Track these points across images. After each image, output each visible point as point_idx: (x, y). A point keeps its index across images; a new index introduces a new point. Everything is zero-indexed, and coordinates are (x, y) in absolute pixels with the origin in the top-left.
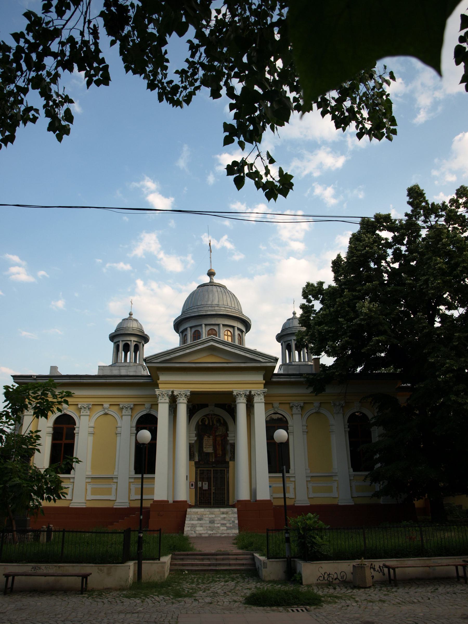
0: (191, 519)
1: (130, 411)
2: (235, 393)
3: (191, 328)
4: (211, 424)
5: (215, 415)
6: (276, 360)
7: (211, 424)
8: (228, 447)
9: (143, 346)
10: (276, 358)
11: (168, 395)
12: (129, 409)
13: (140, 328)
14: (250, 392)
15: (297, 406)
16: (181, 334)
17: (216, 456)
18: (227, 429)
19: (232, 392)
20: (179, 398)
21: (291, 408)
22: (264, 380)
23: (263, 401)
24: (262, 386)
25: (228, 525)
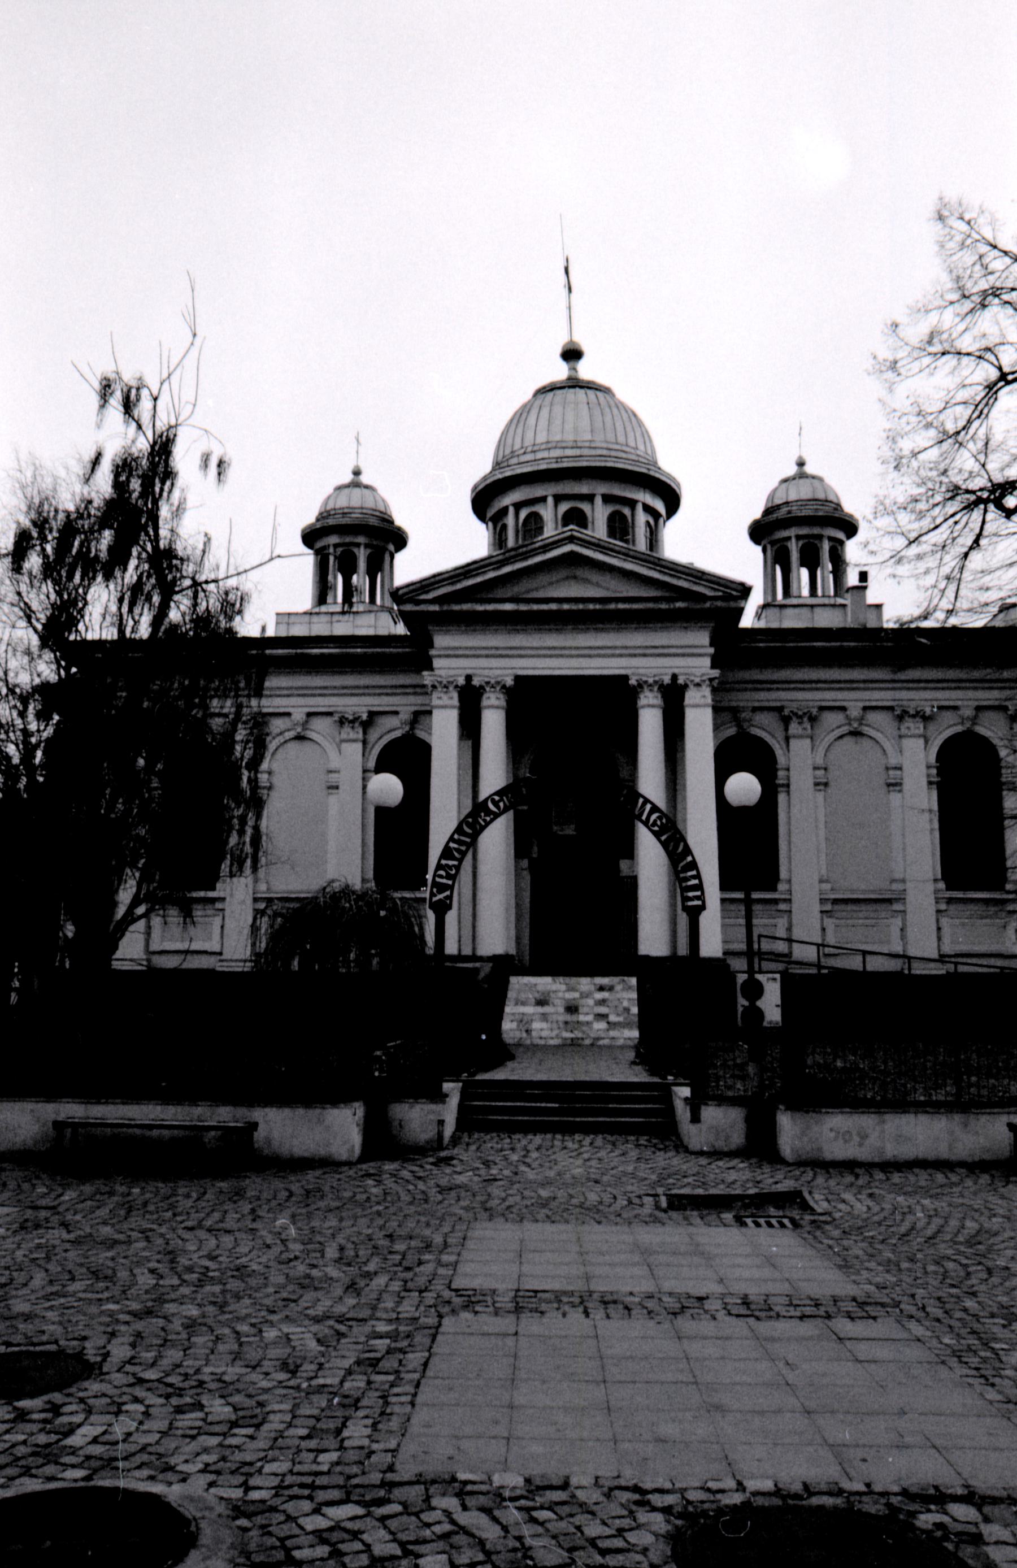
0: (518, 1002)
1: (361, 731)
2: (633, 682)
3: (518, 506)
6: (745, 591)
9: (392, 557)
10: (742, 584)
12: (357, 725)
13: (382, 509)
14: (674, 677)
15: (800, 717)
16: (490, 524)
19: (626, 678)
20: (485, 696)
21: (786, 721)
23: (709, 700)
24: (707, 662)
25: (613, 1018)
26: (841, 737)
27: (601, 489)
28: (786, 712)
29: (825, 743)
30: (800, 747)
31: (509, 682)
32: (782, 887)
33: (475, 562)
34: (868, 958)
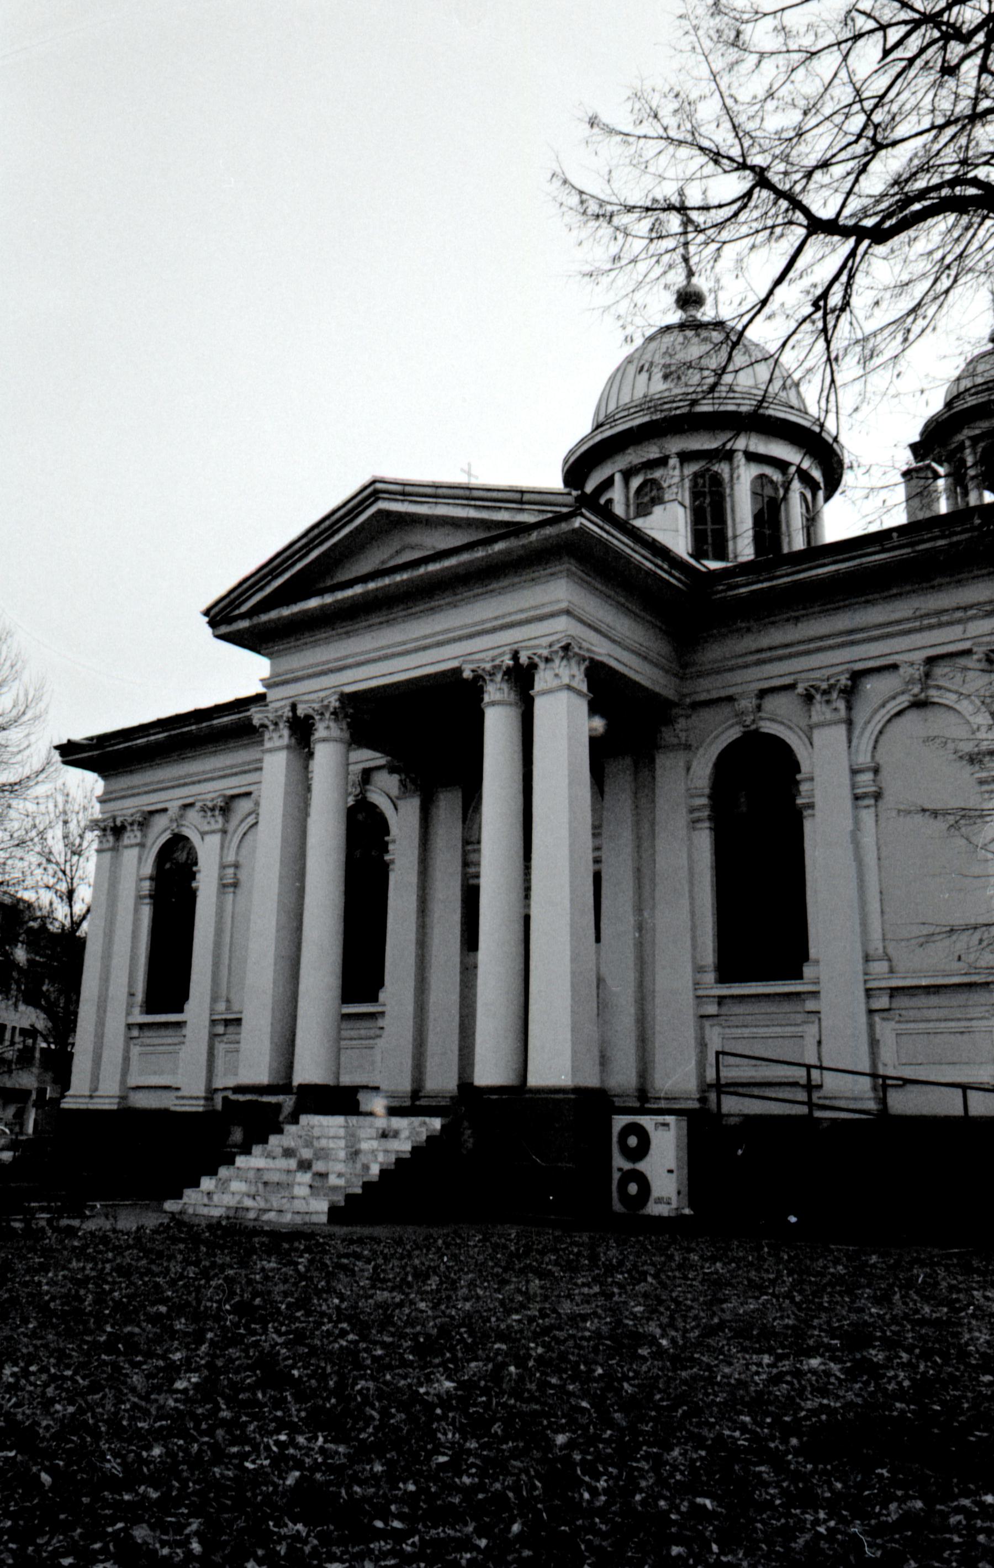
2: (467, 674)
14: (515, 656)
19: (457, 671)
26: (899, 714)
27: (675, 445)
29: (875, 726)
31: (334, 703)
32: (808, 971)
34: (972, 1095)
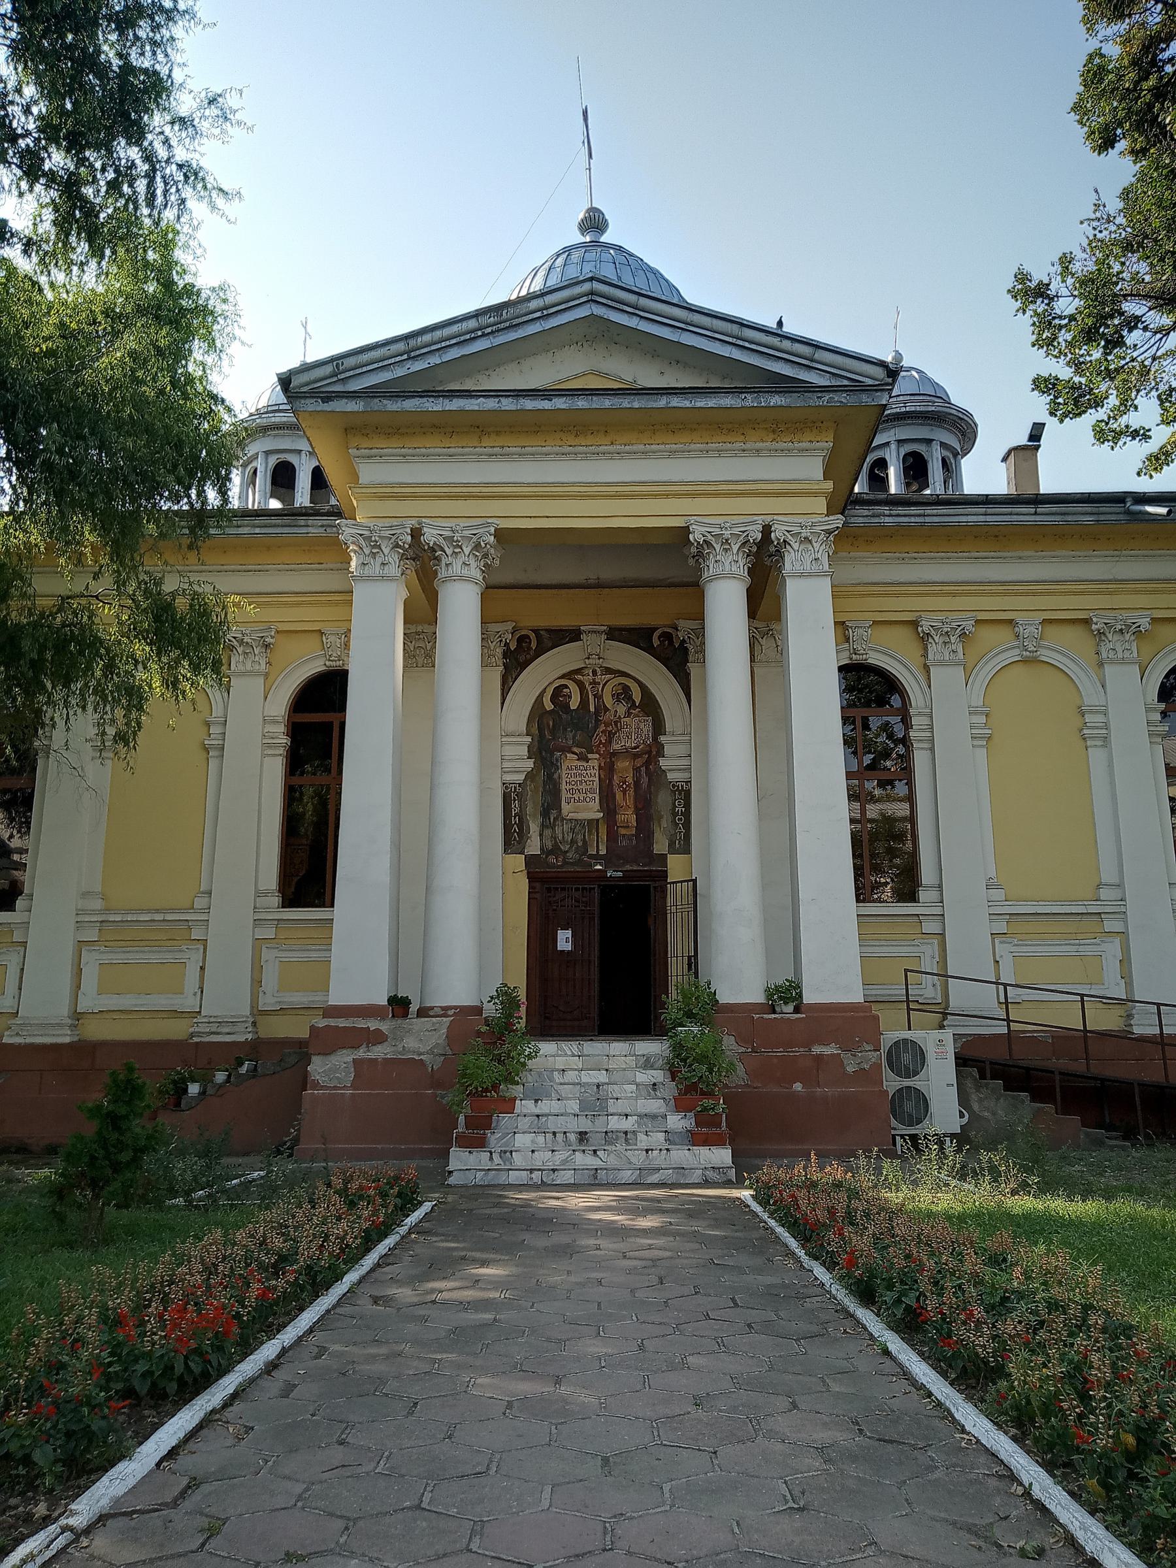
2: (696, 536)
4: (592, 709)
5: (608, 671)
7: (592, 709)
8: (663, 800)
11: (397, 546)
14: (767, 530)
17: (612, 836)
18: (659, 727)
22: (826, 477)
24: (821, 505)
28: (925, 626)
30: (946, 678)
33: (427, 327)
